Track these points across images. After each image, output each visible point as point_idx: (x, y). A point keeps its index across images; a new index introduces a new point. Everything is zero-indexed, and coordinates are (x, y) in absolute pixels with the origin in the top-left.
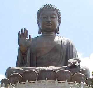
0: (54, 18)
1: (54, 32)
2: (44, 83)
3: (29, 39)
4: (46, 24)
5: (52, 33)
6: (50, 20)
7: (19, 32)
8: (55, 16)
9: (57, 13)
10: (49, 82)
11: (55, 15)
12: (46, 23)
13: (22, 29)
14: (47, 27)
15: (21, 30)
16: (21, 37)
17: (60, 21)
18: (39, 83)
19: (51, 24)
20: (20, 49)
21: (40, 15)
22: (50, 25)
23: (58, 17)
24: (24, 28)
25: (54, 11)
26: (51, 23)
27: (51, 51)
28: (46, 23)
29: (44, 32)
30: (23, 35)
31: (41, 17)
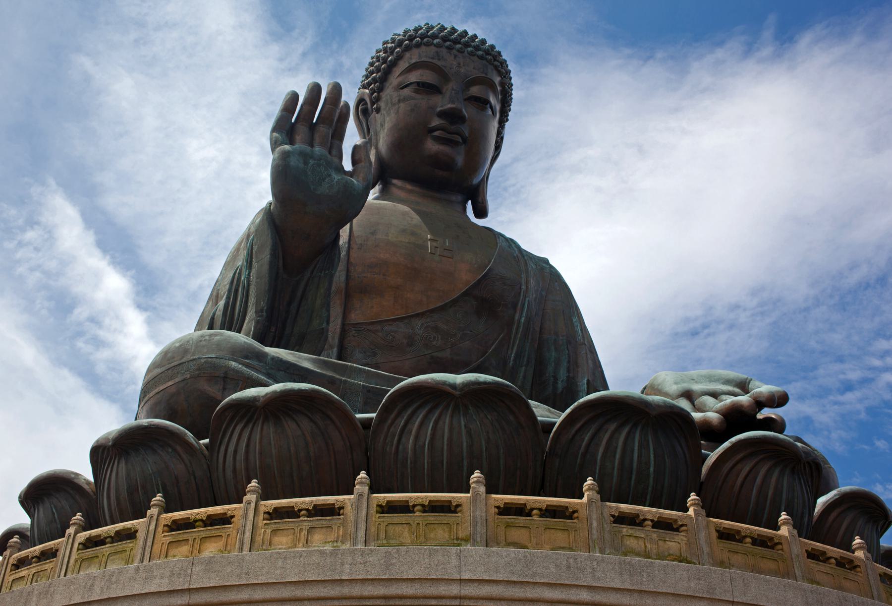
0: (483, 103)
1: (460, 198)
2: (681, 537)
3: (347, 165)
5: (454, 198)
8: (493, 100)
9: (502, 84)
10: (725, 535)
11: (491, 86)
12: (436, 122)
13: (315, 90)
14: (432, 146)
16: (298, 138)
17: (498, 148)
18: (625, 530)
19: (465, 141)
21: (394, 64)
25: (490, 67)
26: (465, 130)
27: (454, 302)
28: (436, 122)
29: (395, 181)
30: (312, 127)
31: (394, 79)
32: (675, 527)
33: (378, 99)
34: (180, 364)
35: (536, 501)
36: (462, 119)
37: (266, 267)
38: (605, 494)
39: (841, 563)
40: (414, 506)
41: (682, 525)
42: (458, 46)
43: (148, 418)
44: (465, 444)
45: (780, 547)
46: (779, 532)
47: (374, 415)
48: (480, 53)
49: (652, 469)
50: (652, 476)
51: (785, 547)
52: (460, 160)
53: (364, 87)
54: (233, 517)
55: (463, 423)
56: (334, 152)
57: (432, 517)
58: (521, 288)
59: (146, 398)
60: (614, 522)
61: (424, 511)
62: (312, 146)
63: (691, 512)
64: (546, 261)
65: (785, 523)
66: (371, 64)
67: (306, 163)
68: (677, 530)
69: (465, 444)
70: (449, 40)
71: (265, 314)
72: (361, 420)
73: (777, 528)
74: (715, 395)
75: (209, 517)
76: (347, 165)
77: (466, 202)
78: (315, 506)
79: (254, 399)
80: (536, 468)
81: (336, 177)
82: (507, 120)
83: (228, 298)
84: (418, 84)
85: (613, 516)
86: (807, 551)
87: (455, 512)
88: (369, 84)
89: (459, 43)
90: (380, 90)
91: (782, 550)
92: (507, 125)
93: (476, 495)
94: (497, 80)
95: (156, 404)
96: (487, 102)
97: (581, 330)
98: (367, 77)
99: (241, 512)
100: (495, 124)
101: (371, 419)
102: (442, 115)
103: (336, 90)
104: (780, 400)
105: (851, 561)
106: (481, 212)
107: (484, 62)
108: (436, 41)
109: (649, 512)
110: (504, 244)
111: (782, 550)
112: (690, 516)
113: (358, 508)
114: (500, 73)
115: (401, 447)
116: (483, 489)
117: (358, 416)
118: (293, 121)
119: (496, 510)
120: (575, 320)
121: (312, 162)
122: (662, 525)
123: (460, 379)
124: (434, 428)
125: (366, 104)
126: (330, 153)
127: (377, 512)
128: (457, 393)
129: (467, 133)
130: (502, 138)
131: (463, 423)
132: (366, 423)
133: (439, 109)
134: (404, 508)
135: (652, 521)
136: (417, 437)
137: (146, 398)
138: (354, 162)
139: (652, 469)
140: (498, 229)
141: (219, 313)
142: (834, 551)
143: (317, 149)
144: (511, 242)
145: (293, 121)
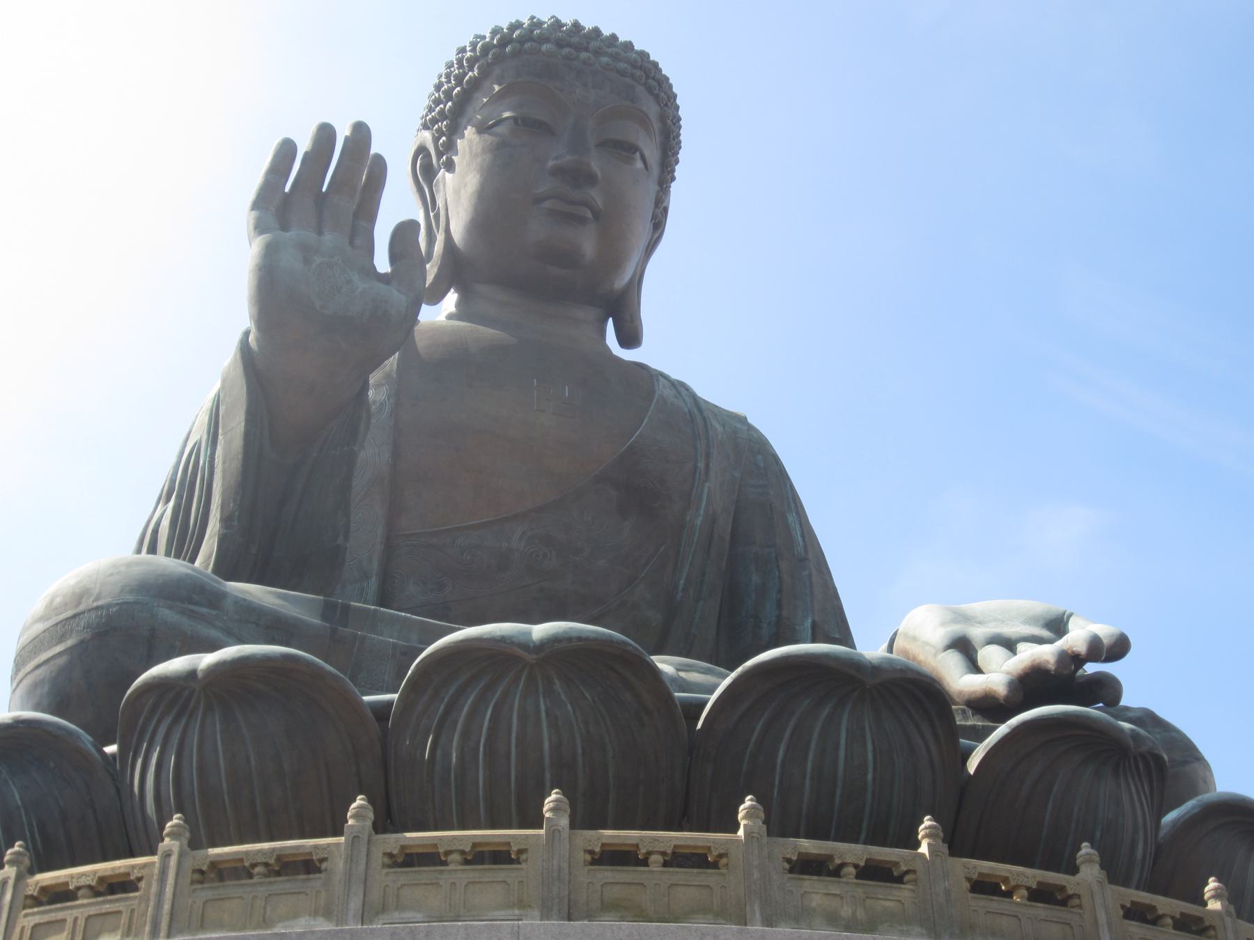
0: (627, 150)
2: (903, 893)
3: (382, 264)
4: (538, 200)
6: (595, 164)
7: (286, 150)
9: (663, 118)
10: (983, 887)
11: (644, 121)
13: (325, 134)
15: (304, 145)
17: (658, 225)
19: (597, 215)
20: (252, 363)
22: (589, 214)
23: (655, 170)
24: (361, 133)
26: (596, 196)
30: (321, 200)
32: (896, 873)
33: (450, 147)
34: (75, 616)
35: (656, 839)
36: (591, 179)
37: (238, 443)
38: (779, 823)
39: (1183, 923)
40: (447, 853)
41: (907, 872)
42: (584, 55)
43: (37, 708)
44: (546, 745)
45: (1076, 901)
46: (1078, 876)
47: (395, 696)
48: (622, 65)
49: (870, 777)
50: (870, 789)
51: (1085, 901)
52: (588, 243)
53: (425, 127)
54: (140, 879)
55: (543, 708)
56: (358, 242)
57: (474, 873)
58: (695, 467)
59: (21, 675)
60: (791, 871)
61: (467, 862)
62: (320, 233)
63: (924, 849)
64: (743, 420)
65: (1089, 860)
66: (438, 87)
67: (307, 261)
68: (899, 880)
69: (546, 745)
70: (569, 45)
71: (236, 523)
72: (371, 704)
73: (1073, 870)
74: (1010, 645)
75: (102, 880)
76: (382, 264)
77: (606, 320)
78: (279, 858)
79: (192, 674)
80: (658, 780)
81: (361, 285)
82: (673, 179)
83: (179, 497)
84: (515, 119)
85: (789, 861)
86: (1123, 907)
87: (518, 861)
88: (434, 121)
89: (586, 49)
90: (454, 131)
91: (1080, 906)
92: (675, 187)
93: (553, 833)
94: (652, 110)
95: (35, 685)
96: (633, 149)
97: (803, 536)
98: (431, 110)
99: (156, 871)
100: (653, 188)
101: (390, 703)
102: (558, 172)
103: (361, 133)
104: (1118, 649)
105: (1199, 920)
106: (630, 337)
107: (628, 80)
108: (545, 47)
109: (853, 852)
110: (669, 393)
111: (1080, 906)
112: (923, 855)
113: (351, 859)
114: (657, 97)
115: (439, 753)
116: (564, 822)
117: (366, 698)
118: (287, 189)
119: (588, 857)
120: (791, 518)
121: (318, 260)
122: (875, 873)
123: (540, 631)
124: (495, 719)
125: (428, 155)
126: (351, 243)
127: (384, 866)
128: (530, 658)
129: (599, 202)
130: (666, 210)
131: (543, 708)
132: (381, 711)
133: (551, 163)
134: (429, 858)
135: (856, 866)
136: (466, 734)
137: (21, 675)
138: (393, 258)
139: (870, 777)
140: (655, 363)
141: (166, 523)
142: (1167, 905)
143: (328, 238)
144: (680, 388)
145: (287, 189)
